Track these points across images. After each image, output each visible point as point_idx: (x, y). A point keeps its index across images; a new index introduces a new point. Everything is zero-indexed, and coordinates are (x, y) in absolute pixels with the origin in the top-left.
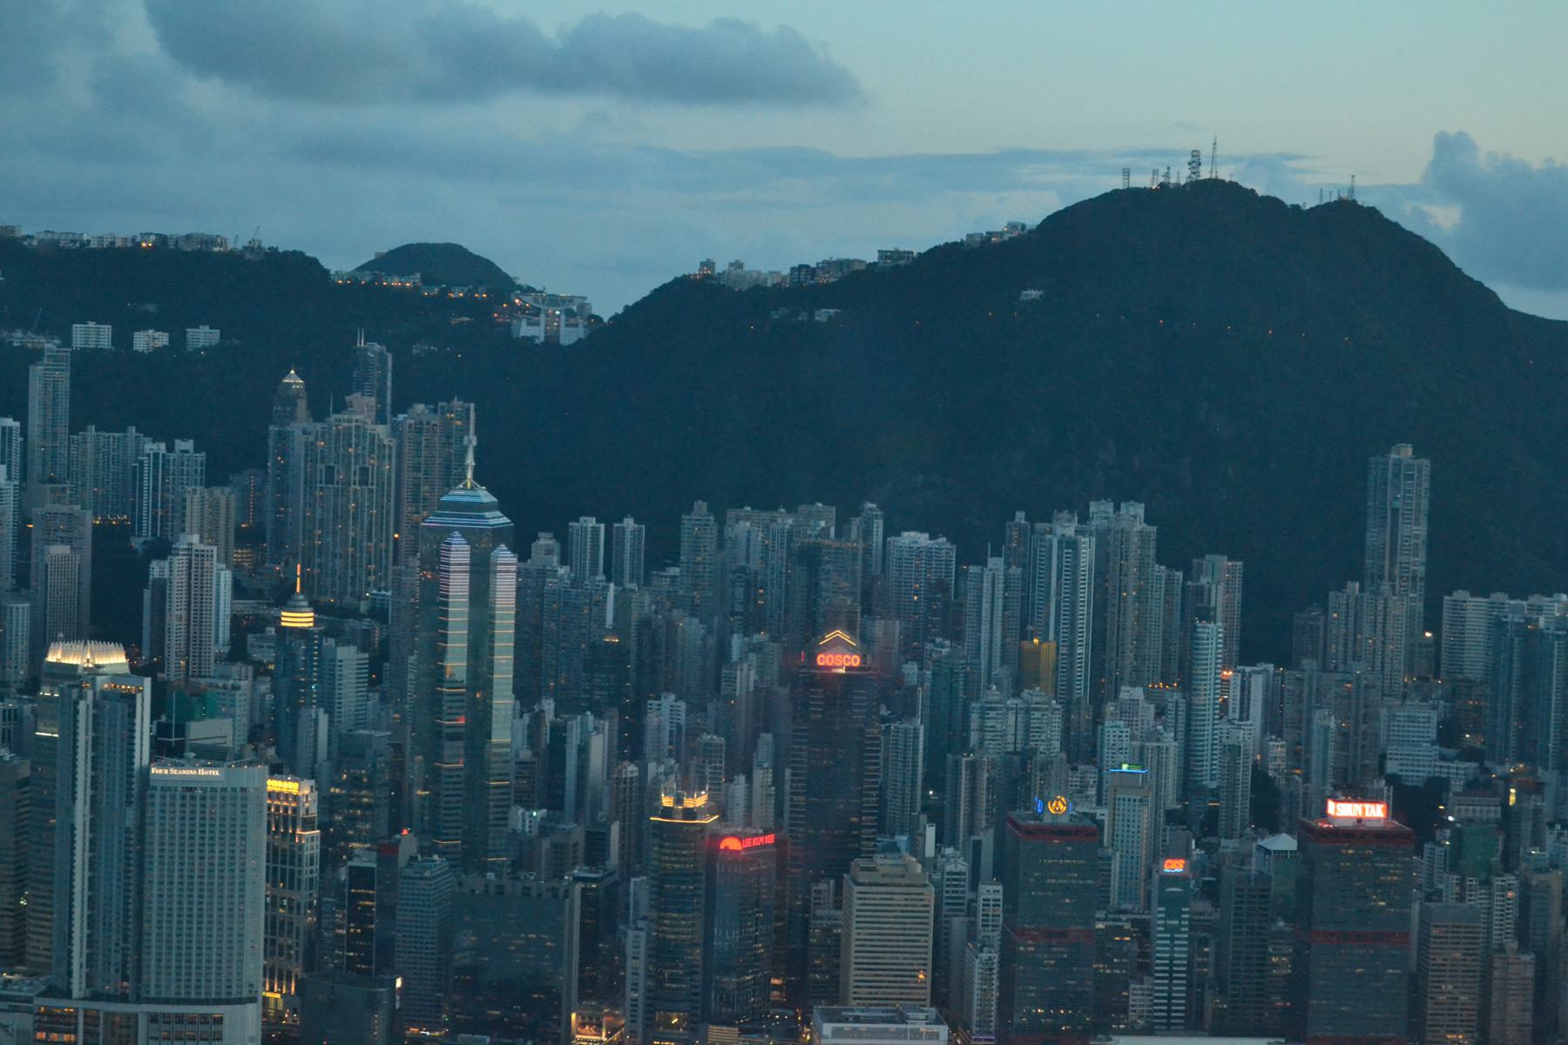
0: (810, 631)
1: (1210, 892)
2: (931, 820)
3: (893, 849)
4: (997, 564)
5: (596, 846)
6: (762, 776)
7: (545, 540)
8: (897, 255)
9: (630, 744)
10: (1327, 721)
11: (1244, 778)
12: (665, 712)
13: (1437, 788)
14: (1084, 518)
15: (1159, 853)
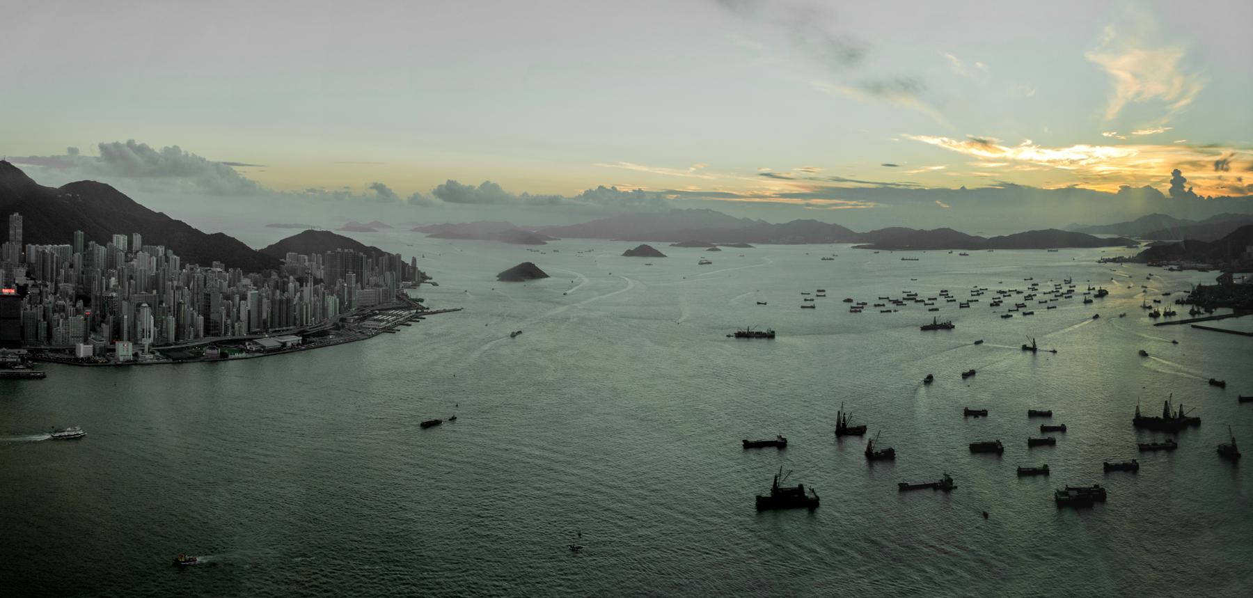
13: (26, 285)
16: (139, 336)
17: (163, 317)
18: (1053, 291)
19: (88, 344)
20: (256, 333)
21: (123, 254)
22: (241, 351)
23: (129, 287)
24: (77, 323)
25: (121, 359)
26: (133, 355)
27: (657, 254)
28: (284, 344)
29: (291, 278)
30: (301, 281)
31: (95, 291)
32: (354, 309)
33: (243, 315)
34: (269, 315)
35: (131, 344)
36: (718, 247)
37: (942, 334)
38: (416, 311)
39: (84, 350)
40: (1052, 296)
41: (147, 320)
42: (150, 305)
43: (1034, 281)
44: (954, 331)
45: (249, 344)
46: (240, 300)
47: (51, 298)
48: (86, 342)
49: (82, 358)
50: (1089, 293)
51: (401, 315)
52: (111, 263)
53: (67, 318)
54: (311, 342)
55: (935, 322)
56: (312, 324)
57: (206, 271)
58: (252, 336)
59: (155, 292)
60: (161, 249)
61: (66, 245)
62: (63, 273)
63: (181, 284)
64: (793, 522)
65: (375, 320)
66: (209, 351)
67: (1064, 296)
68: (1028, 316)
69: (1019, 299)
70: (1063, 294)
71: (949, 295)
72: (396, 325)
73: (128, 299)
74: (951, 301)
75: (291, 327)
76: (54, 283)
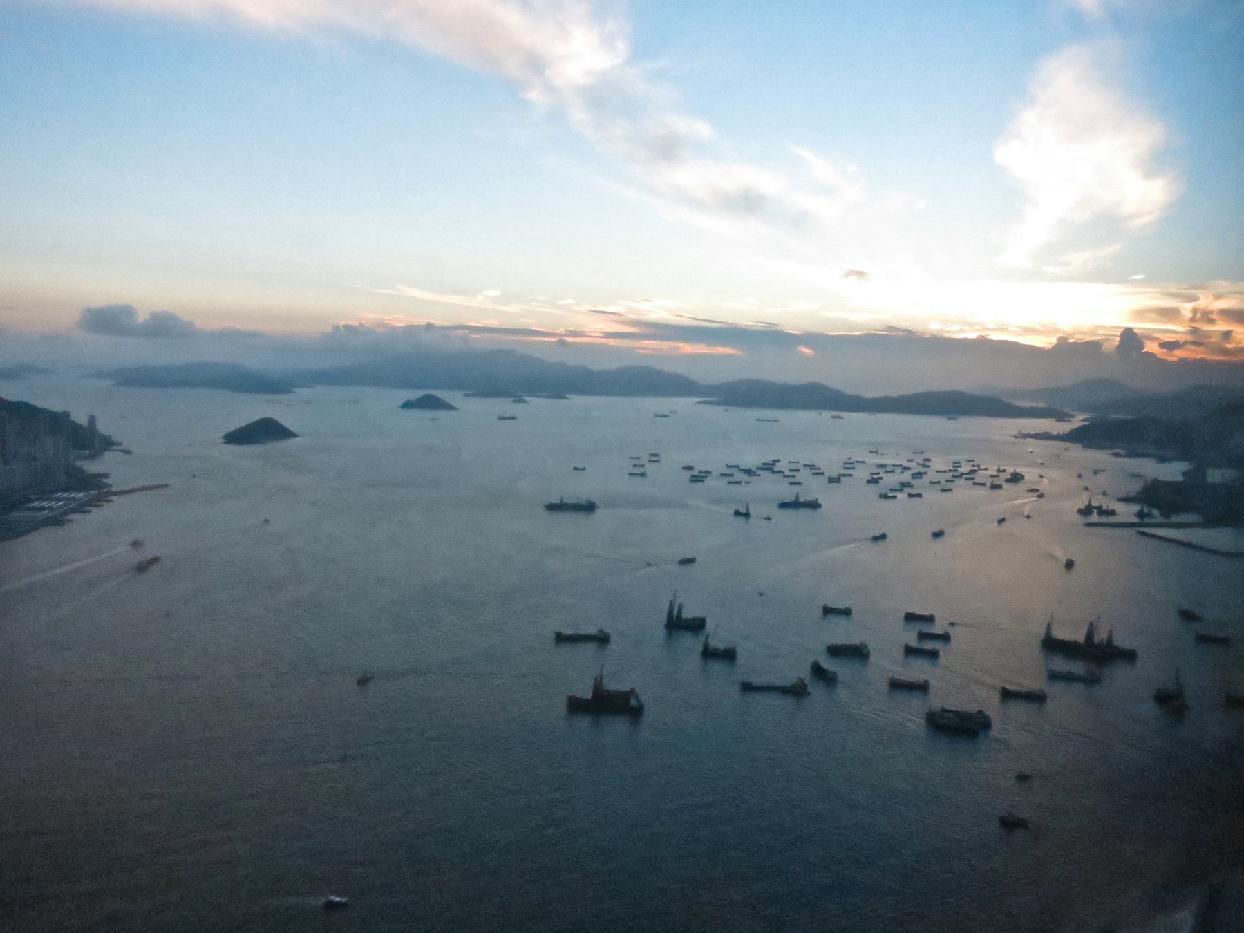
18: (950, 471)
27: (447, 406)
36: (525, 398)
37: (804, 513)
40: (949, 476)
43: (926, 456)
44: (820, 511)
50: (998, 476)
51: (73, 499)
55: (797, 498)
64: (617, 727)
67: (964, 476)
68: (914, 499)
69: (906, 477)
70: (962, 474)
71: (817, 466)
72: (66, 513)
74: (817, 474)
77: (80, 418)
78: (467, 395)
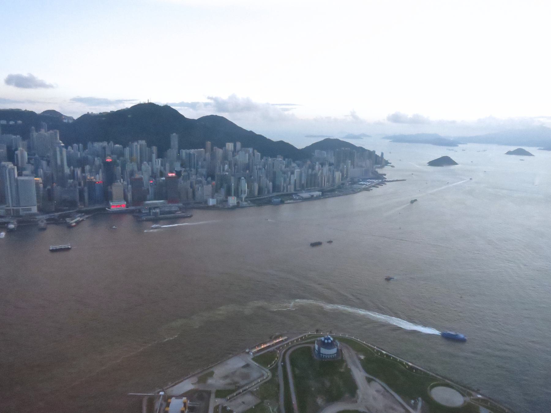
0: (105, 157)
1: (155, 184)
2: (122, 178)
3: (117, 182)
4: (128, 148)
5: (80, 184)
6: (101, 174)
7: (69, 147)
8: (112, 111)
9: (83, 171)
10: (168, 165)
11: (159, 171)
12: (87, 167)
13: (181, 171)
14: (138, 142)
15: (149, 180)
16: (240, 194)
17: (252, 184)
19: (213, 199)
20: (298, 190)
21: (231, 153)
22: (291, 199)
23: (235, 169)
24: (208, 189)
25: (231, 205)
26: (237, 203)
28: (312, 196)
29: (317, 163)
30: (322, 165)
31: (217, 173)
32: (349, 179)
33: (292, 182)
34: (305, 183)
35: (236, 198)
38: (381, 180)
39: (212, 202)
41: (244, 186)
42: (245, 178)
45: (295, 196)
46: (291, 174)
47: (194, 177)
48: (213, 197)
49: (211, 206)
51: (373, 182)
52: (225, 157)
53: (203, 186)
54: (326, 195)
56: (327, 186)
57: (274, 160)
58: (297, 192)
59: (248, 171)
60: (251, 150)
61: (202, 149)
62: (200, 164)
63: (261, 167)
65: (360, 184)
66: (275, 200)
72: (370, 187)
73: (234, 175)
75: (316, 188)
76: (195, 170)
77: (378, 153)
78: (539, 149)
